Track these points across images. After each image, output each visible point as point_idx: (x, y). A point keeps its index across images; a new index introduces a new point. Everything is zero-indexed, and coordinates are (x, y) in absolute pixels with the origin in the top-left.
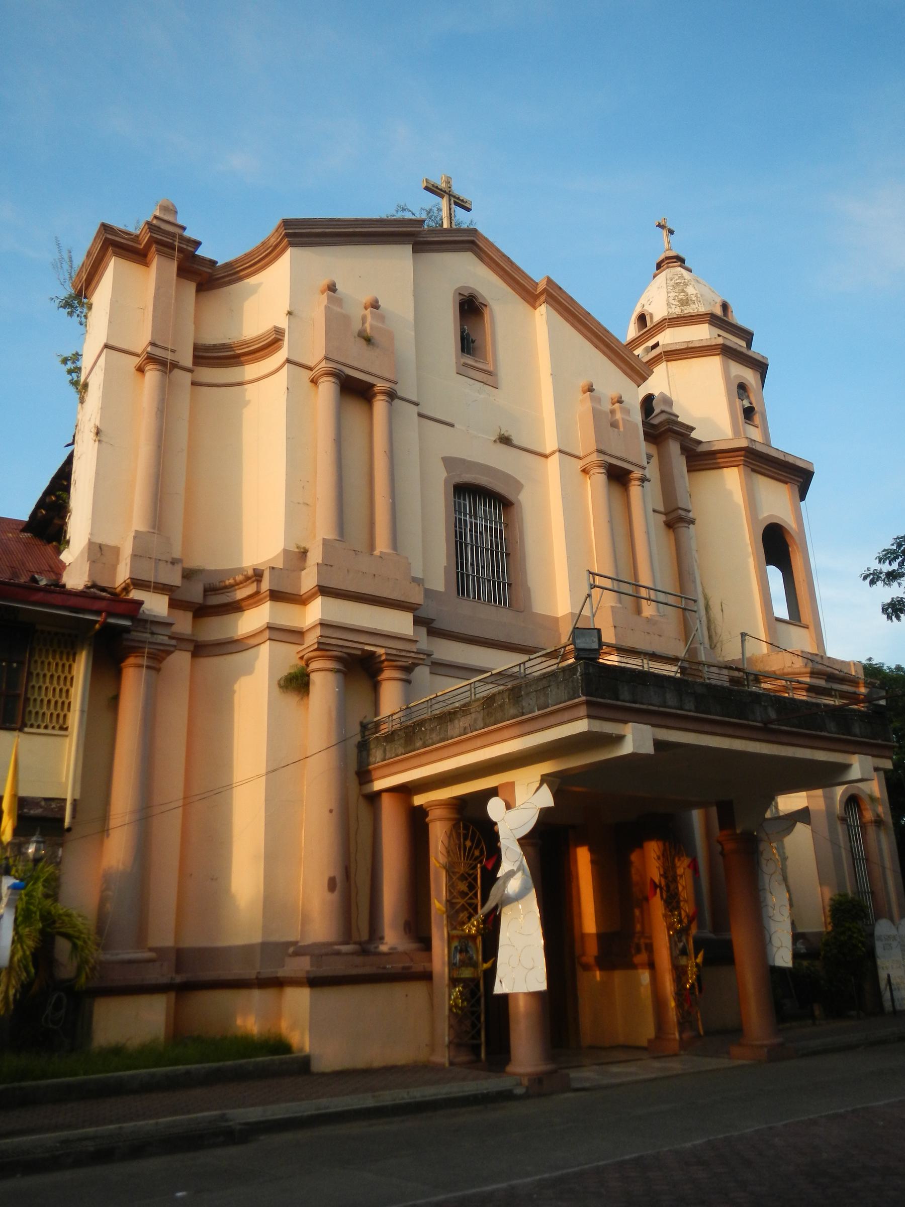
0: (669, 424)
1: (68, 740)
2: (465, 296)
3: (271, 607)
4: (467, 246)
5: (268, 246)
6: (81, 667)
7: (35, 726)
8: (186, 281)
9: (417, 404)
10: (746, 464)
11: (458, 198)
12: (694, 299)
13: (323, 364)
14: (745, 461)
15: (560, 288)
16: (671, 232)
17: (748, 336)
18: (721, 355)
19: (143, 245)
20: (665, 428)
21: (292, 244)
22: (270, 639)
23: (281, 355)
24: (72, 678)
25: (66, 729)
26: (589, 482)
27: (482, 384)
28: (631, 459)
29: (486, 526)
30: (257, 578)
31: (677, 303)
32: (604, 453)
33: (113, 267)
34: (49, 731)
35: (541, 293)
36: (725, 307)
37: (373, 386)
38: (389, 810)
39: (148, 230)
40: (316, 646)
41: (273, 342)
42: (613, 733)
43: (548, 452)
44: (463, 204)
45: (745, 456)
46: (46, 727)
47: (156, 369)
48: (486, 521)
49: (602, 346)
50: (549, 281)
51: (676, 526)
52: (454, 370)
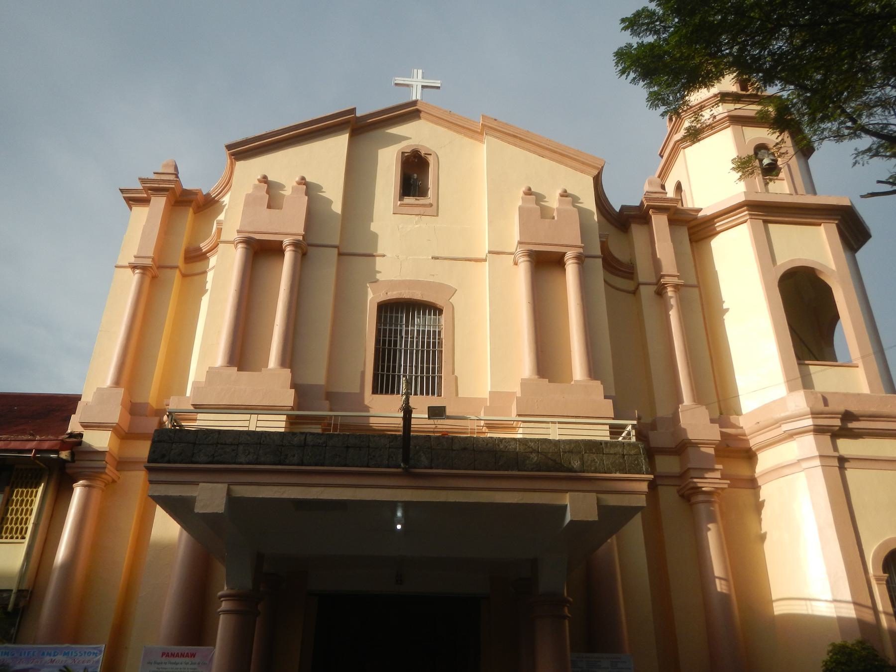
7: (4, 538)
15: (496, 120)
21: (238, 159)
34: (14, 540)
35: (482, 130)
45: (748, 210)
46: (12, 538)
49: (547, 153)
51: (663, 292)
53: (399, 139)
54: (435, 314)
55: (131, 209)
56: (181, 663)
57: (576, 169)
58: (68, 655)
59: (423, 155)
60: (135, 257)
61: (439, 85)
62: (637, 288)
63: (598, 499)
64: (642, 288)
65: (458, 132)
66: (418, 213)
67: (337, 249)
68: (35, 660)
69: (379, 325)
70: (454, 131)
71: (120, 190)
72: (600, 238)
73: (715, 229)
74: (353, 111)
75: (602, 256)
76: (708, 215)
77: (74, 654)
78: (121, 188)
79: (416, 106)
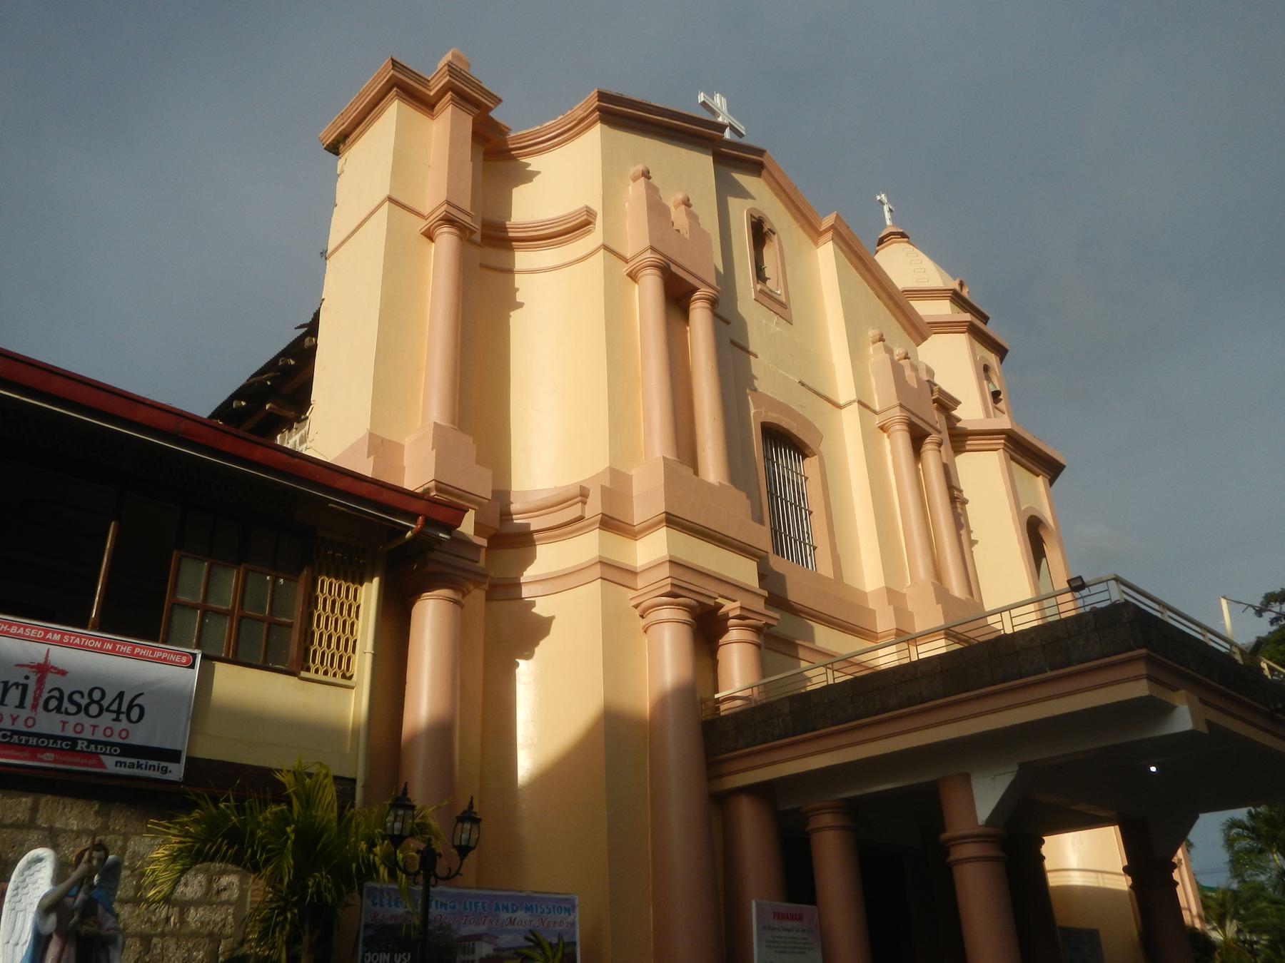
1: (354, 691)
2: (754, 218)
3: (600, 537)
5: (573, 118)
6: (369, 594)
10: (1006, 448)
13: (648, 254)
14: (1005, 444)
15: (848, 227)
17: (985, 319)
18: (967, 333)
19: (432, 93)
22: (602, 578)
23: (594, 238)
24: (358, 607)
25: (351, 677)
26: (887, 442)
30: (583, 498)
33: (394, 110)
35: (826, 231)
36: (961, 285)
38: (749, 819)
39: (447, 72)
40: (668, 589)
41: (580, 225)
43: (842, 402)
45: (1005, 439)
47: (452, 233)
49: (883, 295)
52: (754, 297)
53: (743, 194)
56: (797, 931)
57: (905, 329)
58: (533, 912)
59: (766, 229)
61: (743, 132)
65: (795, 218)
68: (487, 919)
70: (792, 214)
71: (392, 60)
73: (964, 447)
76: (969, 429)
77: (540, 910)
78: (394, 58)
79: (762, 157)
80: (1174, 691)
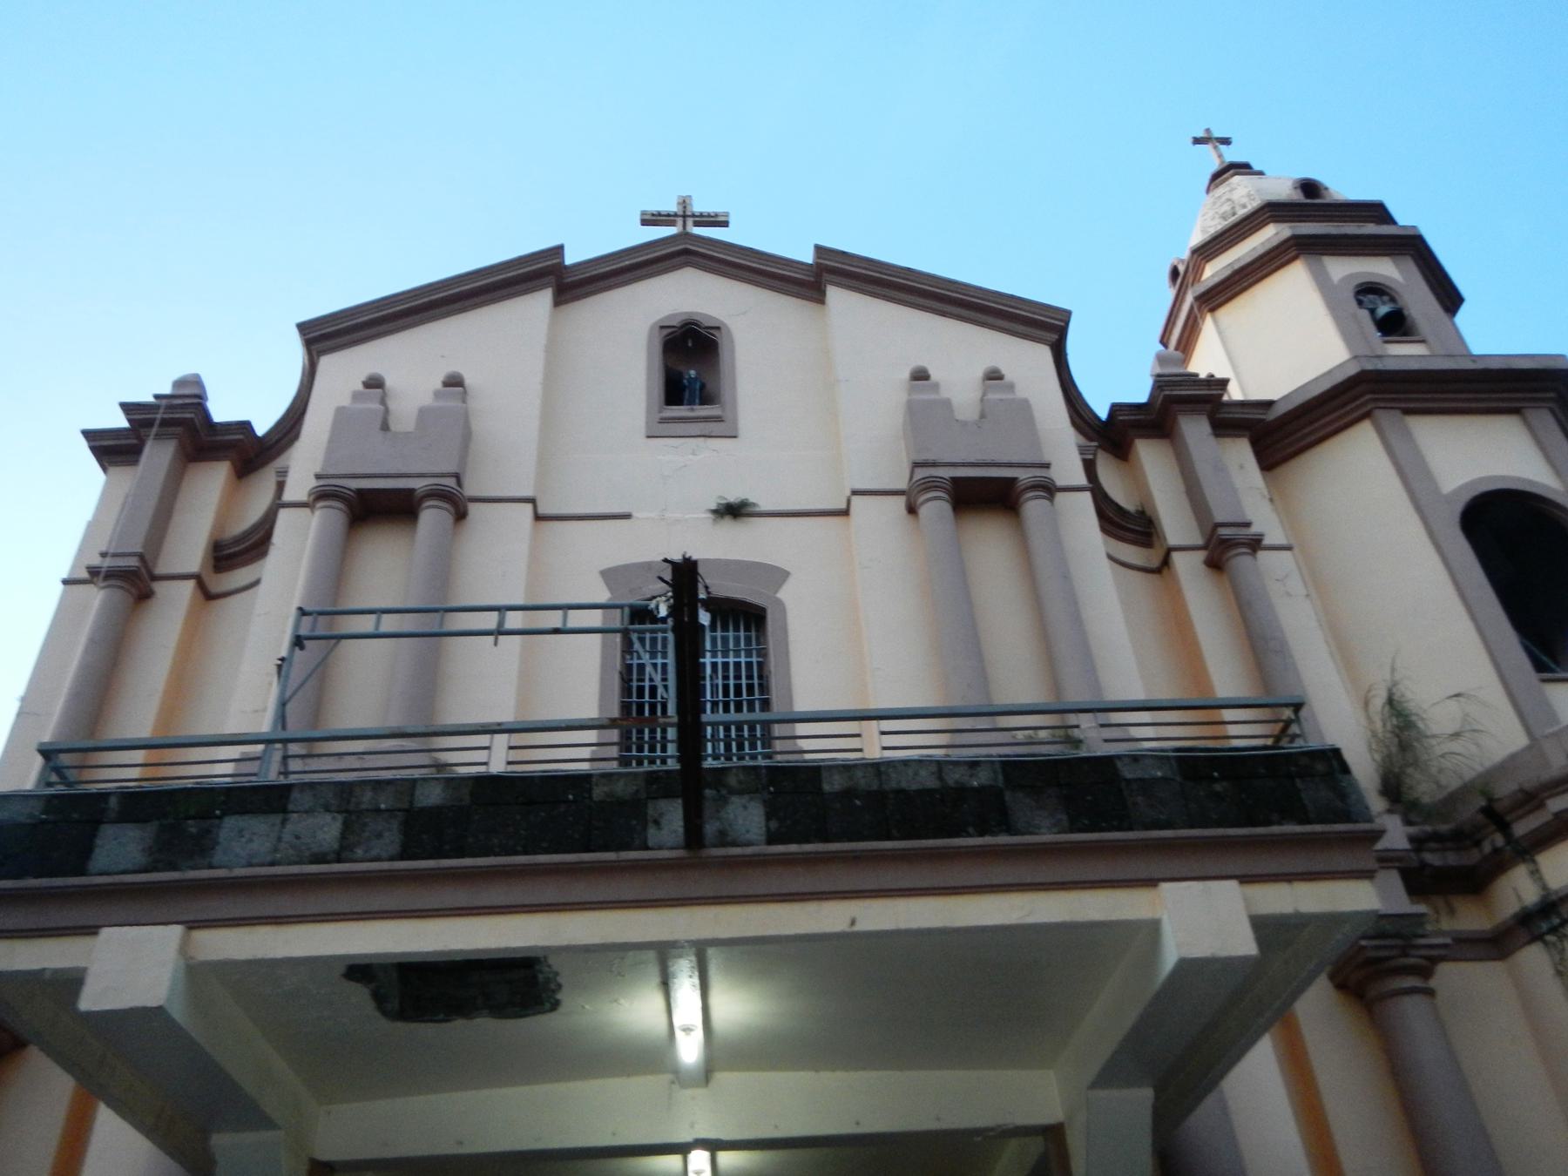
0: (1163, 390)
2: (673, 327)
4: (683, 259)
8: (215, 463)
9: (532, 501)
11: (701, 215)
12: (1244, 200)
15: (844, 253)
16: (1226, 141)
20: (1161, 396)
27: (702, 439)
28: (1015, 459)
29: (714, 665)
31: (1217, 221)
32: (934, 464)
37: (411, 491)
42: (44, 969)
43: (843, 506)
44: (712, 219)
48: (714, 654)
50: (820, 250)
54: (747, 629)
55: (105, 469)
60: (104, 555)
62: (1166, 562)
63: (1246, 900)
64: (1176, 556)
66: (699, 433)
67: (529, 507)
69: (628, 657)
72: (1081, 454)
74: (559, 250)
75: (1091, 486)
80: (96, 934)
